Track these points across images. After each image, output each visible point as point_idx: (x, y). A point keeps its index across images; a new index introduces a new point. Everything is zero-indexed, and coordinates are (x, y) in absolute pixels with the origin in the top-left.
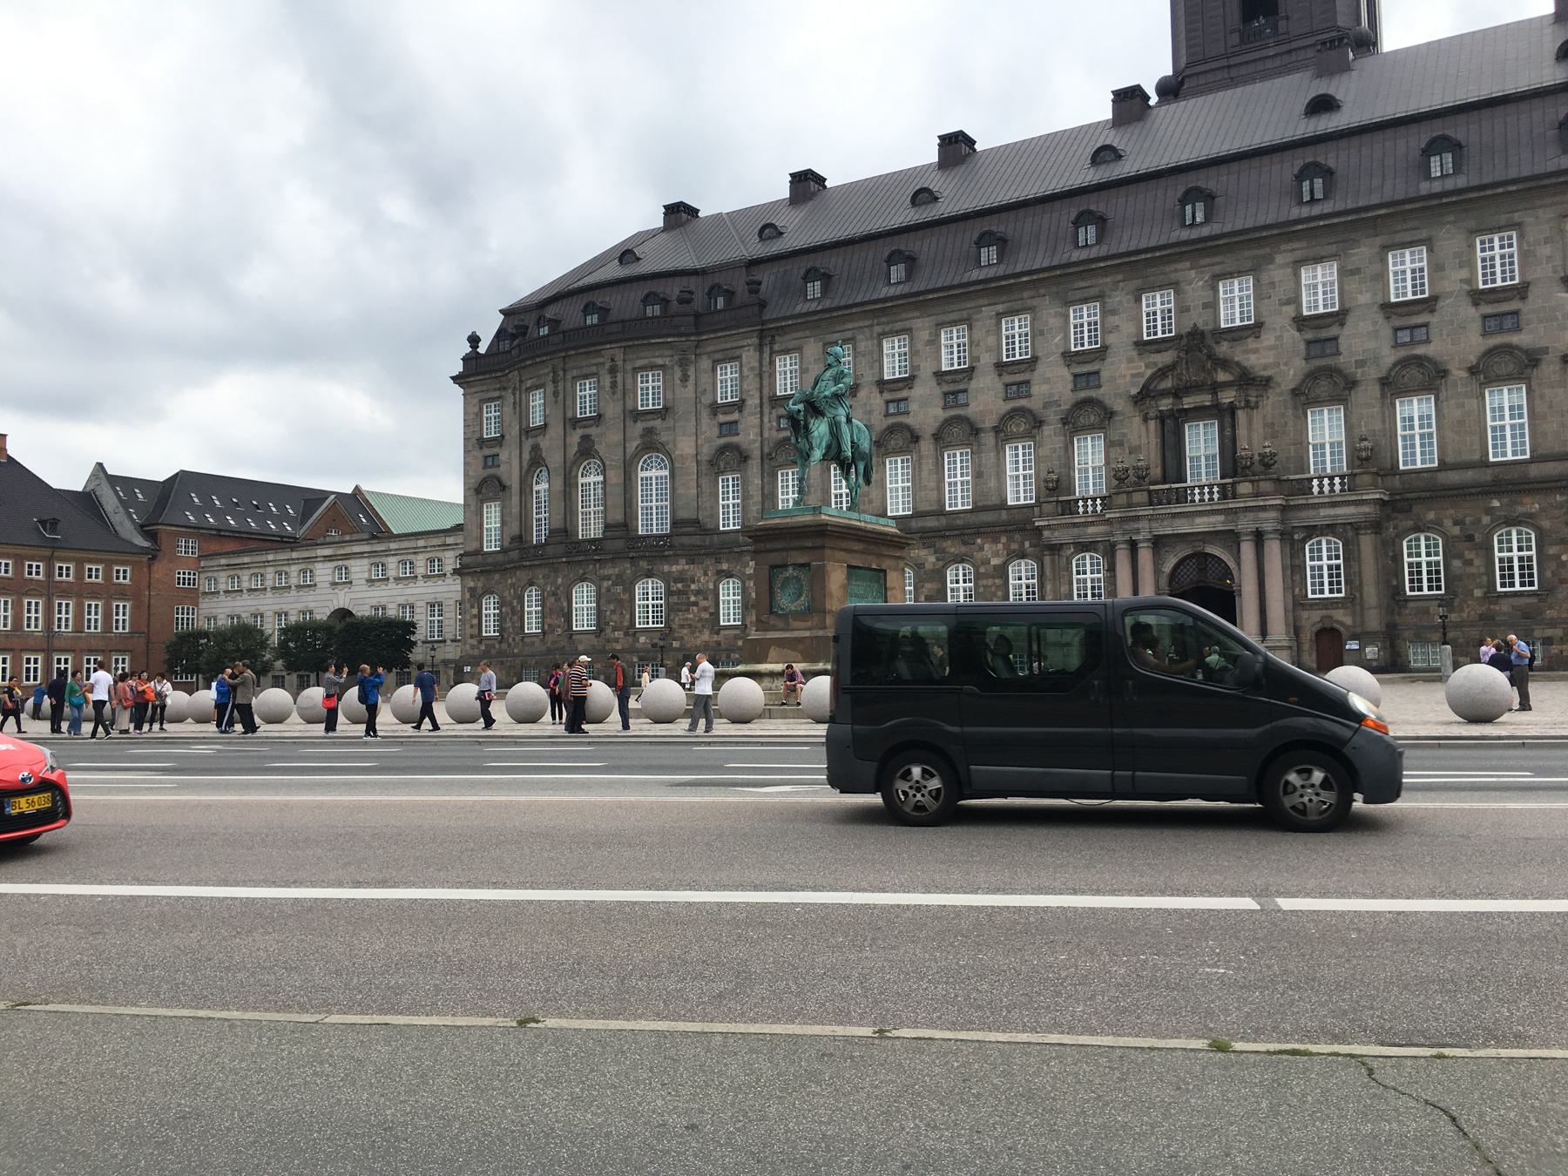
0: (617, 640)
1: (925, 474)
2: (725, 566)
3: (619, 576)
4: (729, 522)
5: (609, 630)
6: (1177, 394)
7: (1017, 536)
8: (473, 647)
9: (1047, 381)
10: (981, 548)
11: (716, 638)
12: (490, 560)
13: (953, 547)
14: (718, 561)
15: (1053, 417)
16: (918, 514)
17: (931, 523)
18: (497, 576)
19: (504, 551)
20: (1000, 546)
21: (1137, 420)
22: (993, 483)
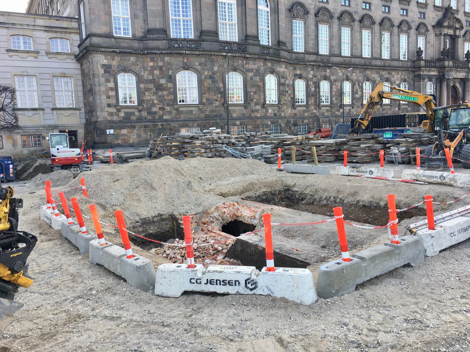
0: (257, 111)
1: (376, 40)
2: (298, 72)
3: (258, 70)
4: (299, 46)
5: (253, 104)
6: (449, 27)
7: (404, 73)
8: (111, 114)
9: (412, 11)
10: (394, 76)
11: (294, 111)
12: (125, 44)
13: (385, 74)
14: (295, 69)
15: (414, 26)
16: (373, 58)
17: (378, 63)
18: (132, 59)
19: (134, 38)
20: (399, 76)
21: (433, 35)
22: (396, 50)
